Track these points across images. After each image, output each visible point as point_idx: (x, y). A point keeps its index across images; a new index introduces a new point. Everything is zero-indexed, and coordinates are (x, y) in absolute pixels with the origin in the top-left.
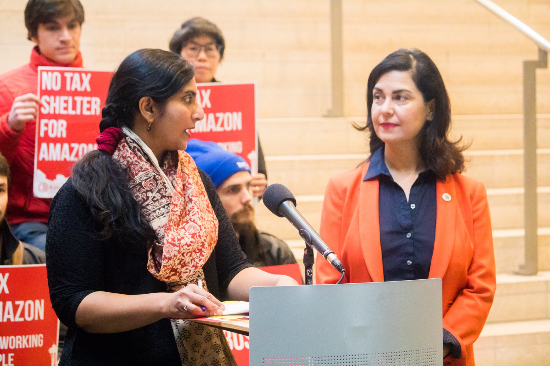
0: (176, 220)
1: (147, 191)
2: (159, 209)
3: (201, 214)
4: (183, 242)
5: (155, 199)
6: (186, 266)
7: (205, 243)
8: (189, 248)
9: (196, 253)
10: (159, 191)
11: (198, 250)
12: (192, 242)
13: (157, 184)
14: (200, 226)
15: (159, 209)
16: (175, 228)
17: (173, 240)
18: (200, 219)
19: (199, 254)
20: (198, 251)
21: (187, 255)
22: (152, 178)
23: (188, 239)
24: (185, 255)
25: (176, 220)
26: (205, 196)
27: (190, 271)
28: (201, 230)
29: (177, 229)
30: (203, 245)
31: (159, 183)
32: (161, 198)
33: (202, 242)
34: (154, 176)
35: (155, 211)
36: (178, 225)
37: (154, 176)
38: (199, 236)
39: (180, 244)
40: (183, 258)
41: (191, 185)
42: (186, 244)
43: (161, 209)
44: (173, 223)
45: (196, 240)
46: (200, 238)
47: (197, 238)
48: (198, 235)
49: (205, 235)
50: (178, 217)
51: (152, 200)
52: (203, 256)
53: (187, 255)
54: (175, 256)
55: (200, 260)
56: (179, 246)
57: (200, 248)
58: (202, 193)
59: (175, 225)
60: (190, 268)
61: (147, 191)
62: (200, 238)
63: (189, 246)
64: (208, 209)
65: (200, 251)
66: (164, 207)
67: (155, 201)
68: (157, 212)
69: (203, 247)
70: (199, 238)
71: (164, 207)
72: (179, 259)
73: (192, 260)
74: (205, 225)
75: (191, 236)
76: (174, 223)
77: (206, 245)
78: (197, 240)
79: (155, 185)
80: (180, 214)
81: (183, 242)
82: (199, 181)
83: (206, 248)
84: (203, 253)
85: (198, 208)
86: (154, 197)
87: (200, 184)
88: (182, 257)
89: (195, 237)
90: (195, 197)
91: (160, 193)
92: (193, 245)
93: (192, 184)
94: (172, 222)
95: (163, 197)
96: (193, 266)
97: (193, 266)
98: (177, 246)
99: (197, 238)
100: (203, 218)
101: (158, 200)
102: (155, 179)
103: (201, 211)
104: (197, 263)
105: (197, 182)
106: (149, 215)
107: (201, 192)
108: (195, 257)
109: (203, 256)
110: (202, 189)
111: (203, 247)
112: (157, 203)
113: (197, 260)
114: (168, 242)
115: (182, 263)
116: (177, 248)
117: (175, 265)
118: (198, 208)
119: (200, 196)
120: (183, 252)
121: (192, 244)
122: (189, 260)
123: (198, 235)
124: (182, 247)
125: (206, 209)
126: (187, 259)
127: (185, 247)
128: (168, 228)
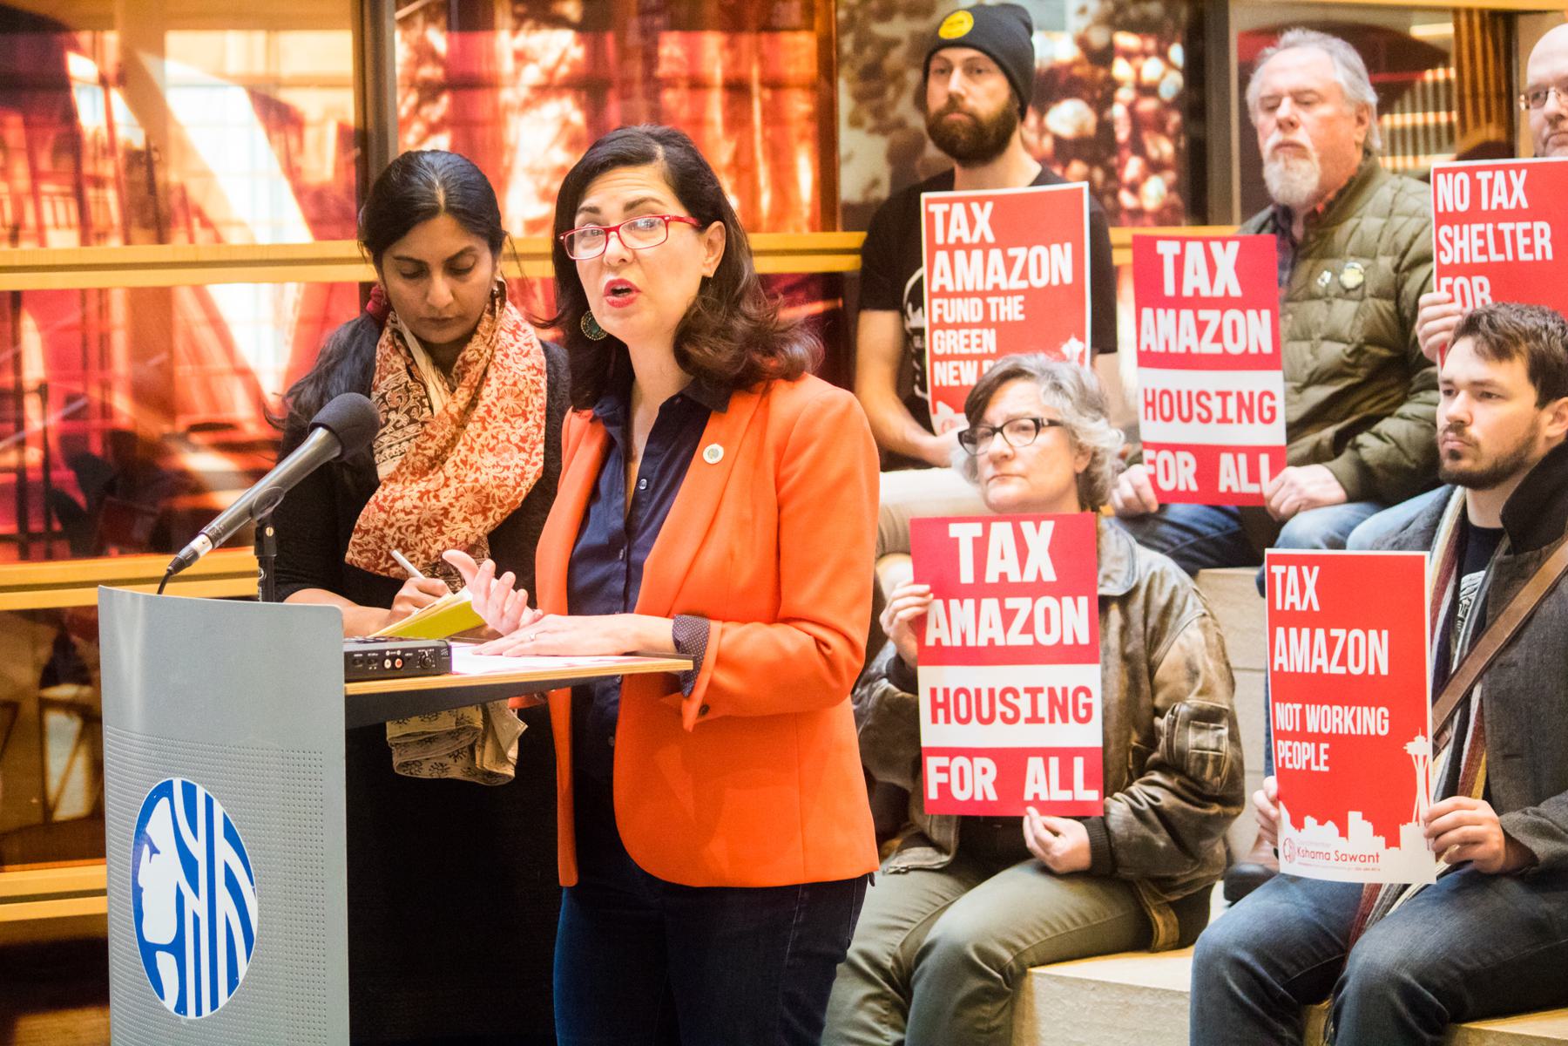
0: (418, 464)
1: (391, 409)
2: (400, 443)
3: (466, 456)
4: (399, 505)
5: (398, 425)
6: (409, 550)
7: (451, 509)
8: (409, 517)
9: (430, 526)
10: (408, 412)
11: (435, 521)
12: (415, 507)
13: (409, 399)
14: (447, 479)
15: (400, 443)
16: (410, 477)
17: (385, 499)
18: (456, 465)
19: (435, 530)
20: (435, 524)
21: (407, 530)
22: (403, 387)
23: (408, 503)
24: (403, 531)
25: (418, 464)
26: (527, 420)
27: (418, 560)
28: (446, 485)
29: (412, 481)
30: (446, 512)
31: (411, 396)
32: (408, 424)
33: (444, 508)
34: (407, 382)
35: (390, 446)
36: (426, 474)
37: (407, 382)
38: (436, 497)
39: (391, 508)
40: (402, 537)
41: (482, 399)
42: (403, 510)
43: (403, 444)
44: (411, 469)
45: (425, 504)
46: (439, 501)
47: (429, 500)
48: (431, 495)
49: (453, 494)
50: (426, 460)
51: (394, 426)
52: (443, 533)
53: (407, 530)
54: (376, 528)
55: (435, 541)
56: (389, 512)
57: (440, 518)
58: (524, 414)
59: (413, 474)
60: (419, 555)
61: (391, 409)
62: (439, 501)
63: (407, 514)
64: (520, 444)
65: (440, 523)
66: (409, 440)
67: (396, 429)
68: (394, 448)
69: (447, 518)
70: (433, 501)
71: (409, 440)
72: (393, 539)
73: (421, 540)
74: (466, 476)
75: (418, 495)
76: (414, 468)
77: (454, 512)
78: (429, 504)
79: (404, 399)
80: (433, 455)
81: (399, 505)
82: (526, 392)
83: (453, 518)
84: (444, 529)
85: (465, 444)
86: (398, 421)
87: (527, 399)
88: (398, 536)
89: (425, 497)
90: (474, 422)
91: (409, 415)
92: (420, 514)
93: (484, 397)
94: (407, 468)
95: (413, 421)
96: (423, 552)
97: (423, 552)
98: (385, 512)
99: (429, 500)
100: (470, 462)
101: (402, 427)
102: (408, 390)
103: (472, 449)
104: (430, 547)
105: (522, 392)
106: (381, 452)
107: (520, 412)
108: (427, 534)
109: (443, 533)
110: (527, 406)
111: (447, 518)
112: (399, 434)
113: (430, 541)
114: (375, 501)
115: (403, 544)
116: (383, 516)
117: (390, 548)
118: (465, 444)
119: (512, 420)
120: (398, 525)
121: (416, 511)
122: (417, 540)
123: (431, 495)
124: (394, 514)
125: (516, 445)
126: (411, 539)
127: (401, 515)
128: (392, 478)
